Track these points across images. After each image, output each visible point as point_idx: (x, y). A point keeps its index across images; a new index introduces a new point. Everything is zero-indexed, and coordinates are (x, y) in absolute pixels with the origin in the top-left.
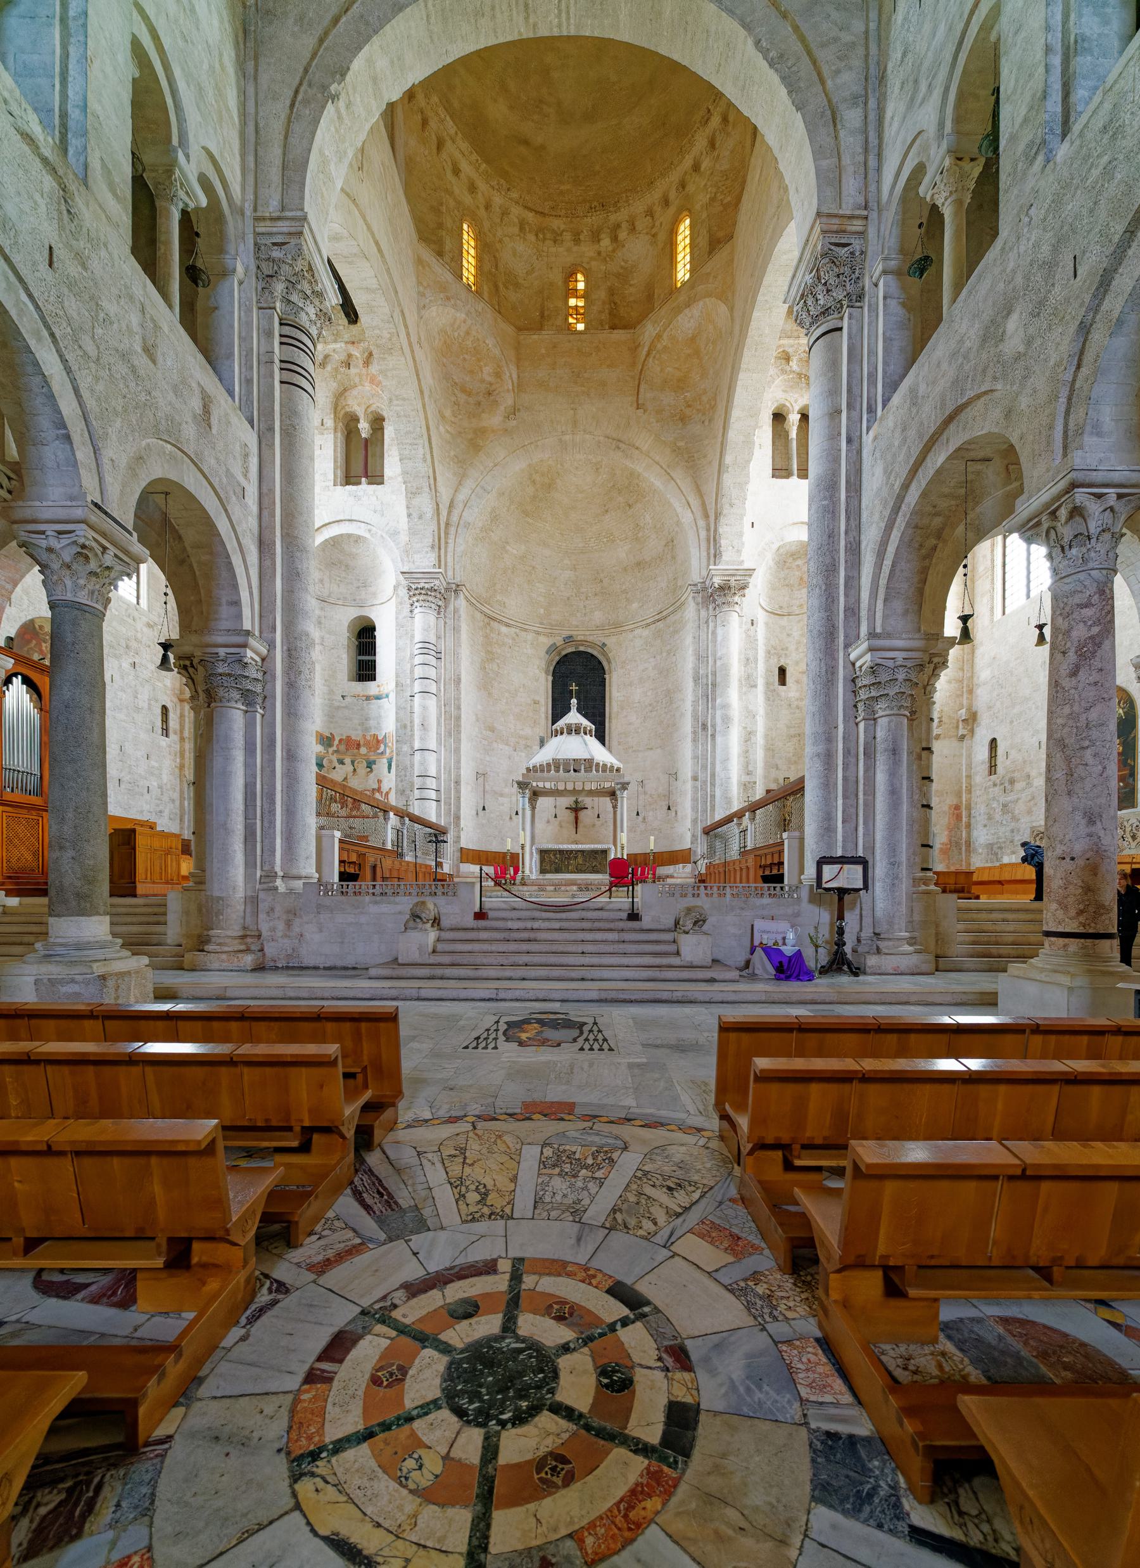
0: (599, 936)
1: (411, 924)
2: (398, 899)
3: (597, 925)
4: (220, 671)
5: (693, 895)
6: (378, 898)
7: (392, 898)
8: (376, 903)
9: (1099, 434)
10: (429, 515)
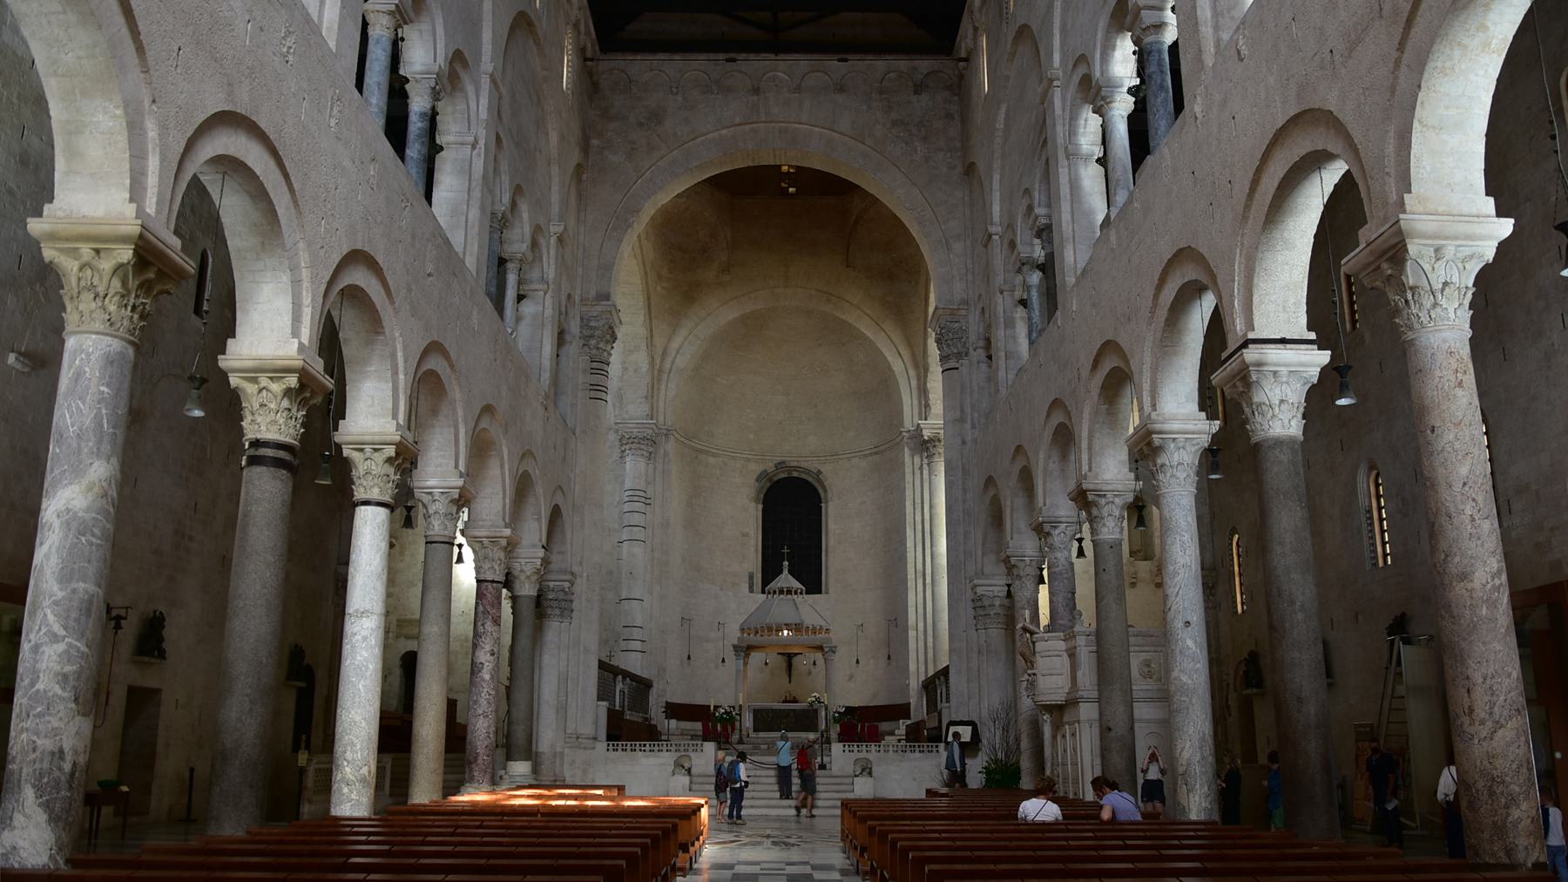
2: (661, 754)
4: (550, 597)
8: (646, 757)
9: (1020, 533)
10: (644, 370)
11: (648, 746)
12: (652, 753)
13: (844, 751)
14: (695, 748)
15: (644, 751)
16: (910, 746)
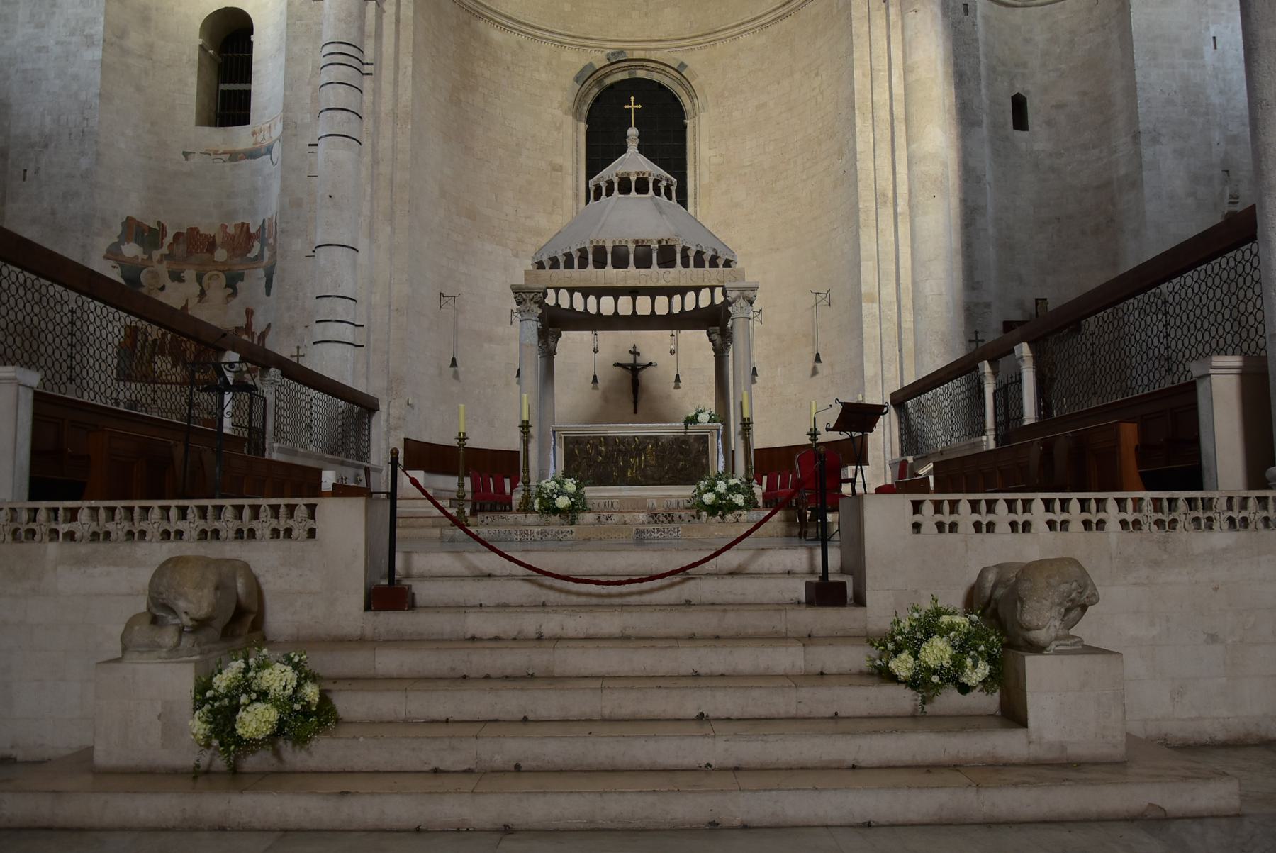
0: (745, 659)
1: (143, 632)
3: (732, 621)
5: (1013, 525)
6: (83, 549)
7: (125, 549)
8: (82, 562)
11: (84, 516)
12: (101, 547)
13: (917, 527)
14: (283, 523)
15: (70, 536)
16: (1156, 501)
